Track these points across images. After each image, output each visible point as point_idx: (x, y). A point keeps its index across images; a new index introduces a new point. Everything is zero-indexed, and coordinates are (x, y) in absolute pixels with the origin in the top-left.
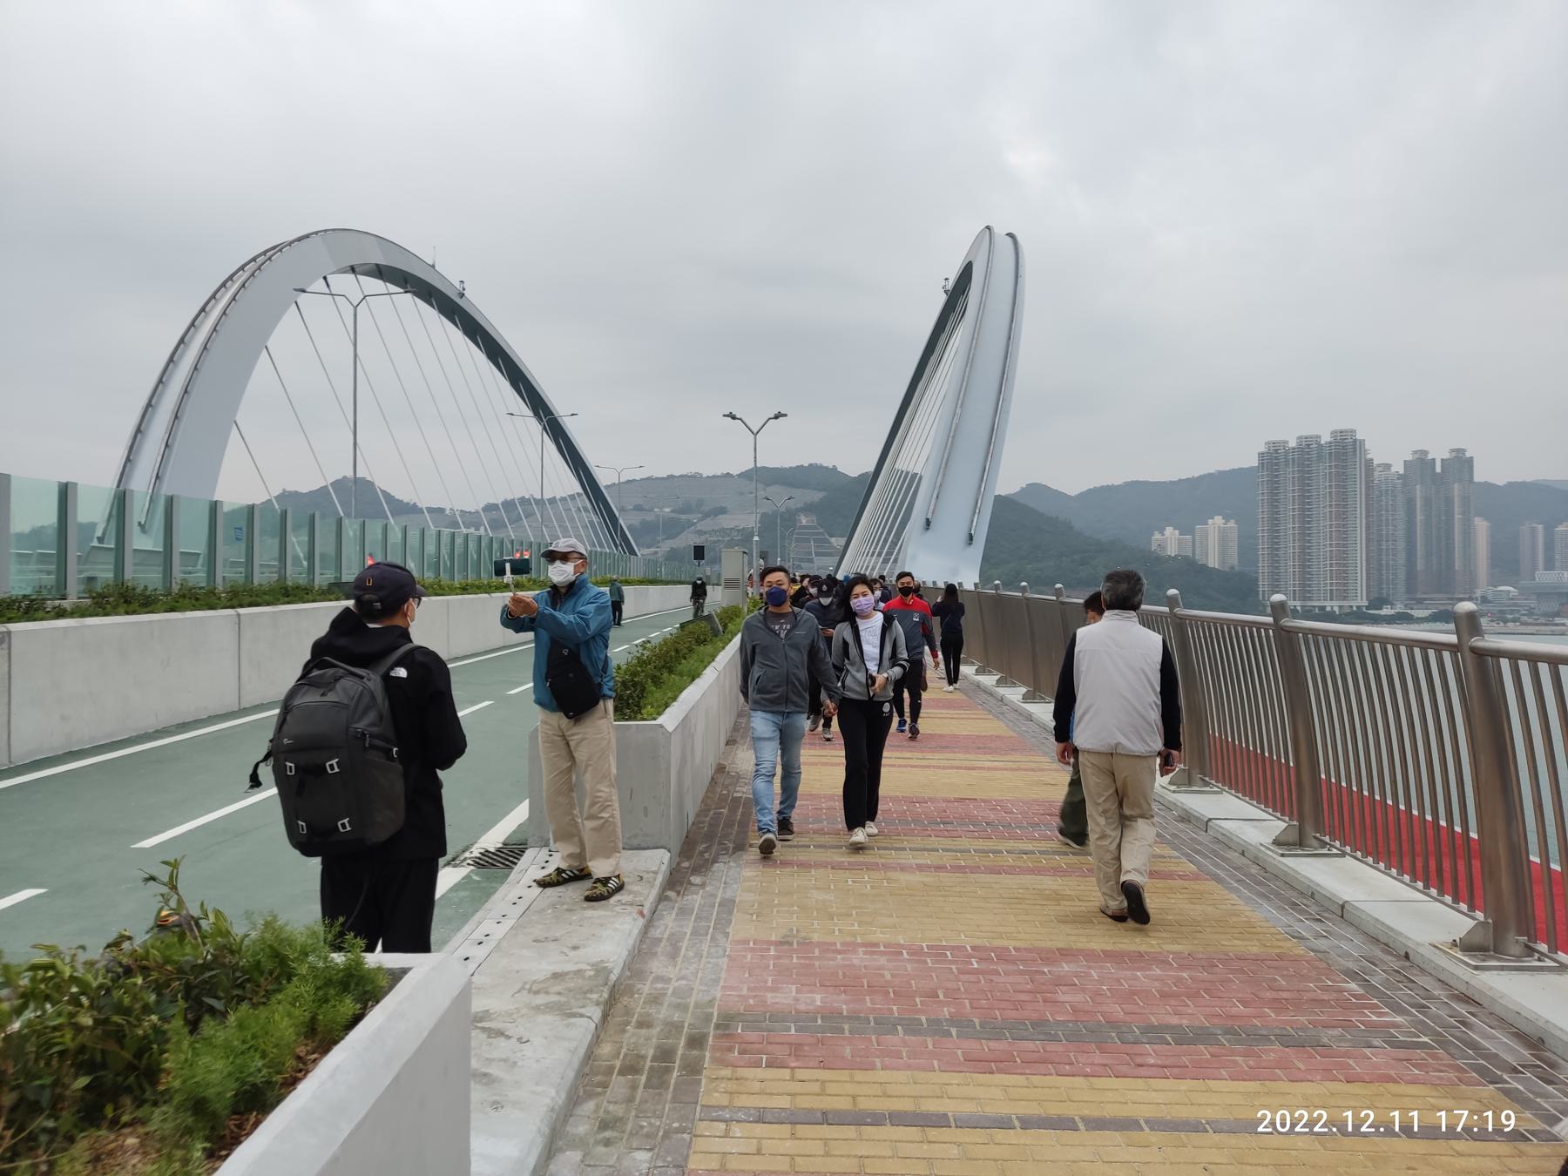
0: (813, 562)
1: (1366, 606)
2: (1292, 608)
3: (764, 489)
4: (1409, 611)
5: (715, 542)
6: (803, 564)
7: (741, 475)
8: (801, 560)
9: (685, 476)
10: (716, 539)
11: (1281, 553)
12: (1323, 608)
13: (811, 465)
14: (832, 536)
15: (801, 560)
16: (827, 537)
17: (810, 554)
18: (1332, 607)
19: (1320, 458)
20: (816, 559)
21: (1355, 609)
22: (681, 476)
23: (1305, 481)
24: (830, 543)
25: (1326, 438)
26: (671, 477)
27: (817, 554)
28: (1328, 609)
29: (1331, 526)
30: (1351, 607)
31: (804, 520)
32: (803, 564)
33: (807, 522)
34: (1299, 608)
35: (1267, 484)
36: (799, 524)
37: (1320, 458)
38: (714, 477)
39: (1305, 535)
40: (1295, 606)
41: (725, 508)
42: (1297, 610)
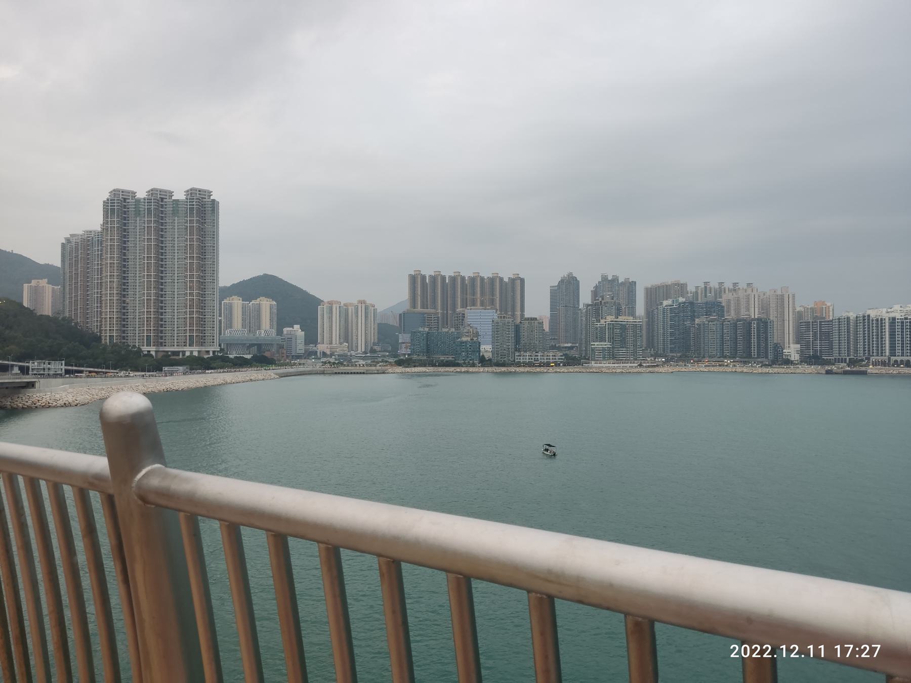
1: (218, 351)
2: (146, 353)
4: (243, 356)
11: (127, 300)
12: (176, 353)
18: (192, 352)
19: (175, 212)
21: (211, 354)
23: (160, 231)
25: (180, 195)
28: (188, 354)
29: (192, 276)
30: (208, 352)
34: (153, 353)
35: (118, 229)
37: (175, 212)
39: (160, 284)
40: (149, 351)
42: (151, 355)
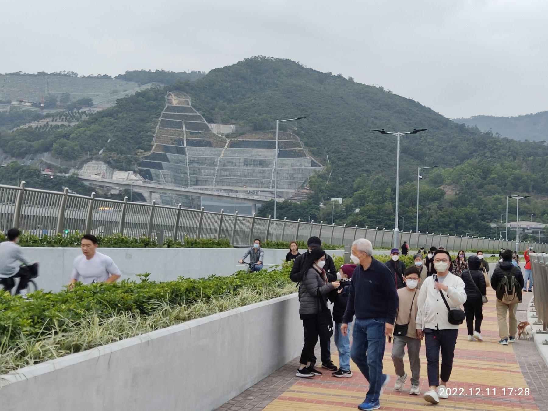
0: (186, 155)
3: (139, 86)
5: (57, 127)
6: (169, 155)
7: (120, 77)
8: (167, 149)
9: (59, 75)
10: (60, 124)
13: (192, 72)
14: (211, 121)
15: (167, 149)
16: (205, 122)
17: (180, 141)
20: (187, 149)
22: (53, 74)
24: (207, 129)
26: (42, 74)
27: (191, 143)
31: (175, 101)
32: (169, 155)
33: (178, 103)
36: (167, 105)
38: (90, 77)
41: (91, 100)
